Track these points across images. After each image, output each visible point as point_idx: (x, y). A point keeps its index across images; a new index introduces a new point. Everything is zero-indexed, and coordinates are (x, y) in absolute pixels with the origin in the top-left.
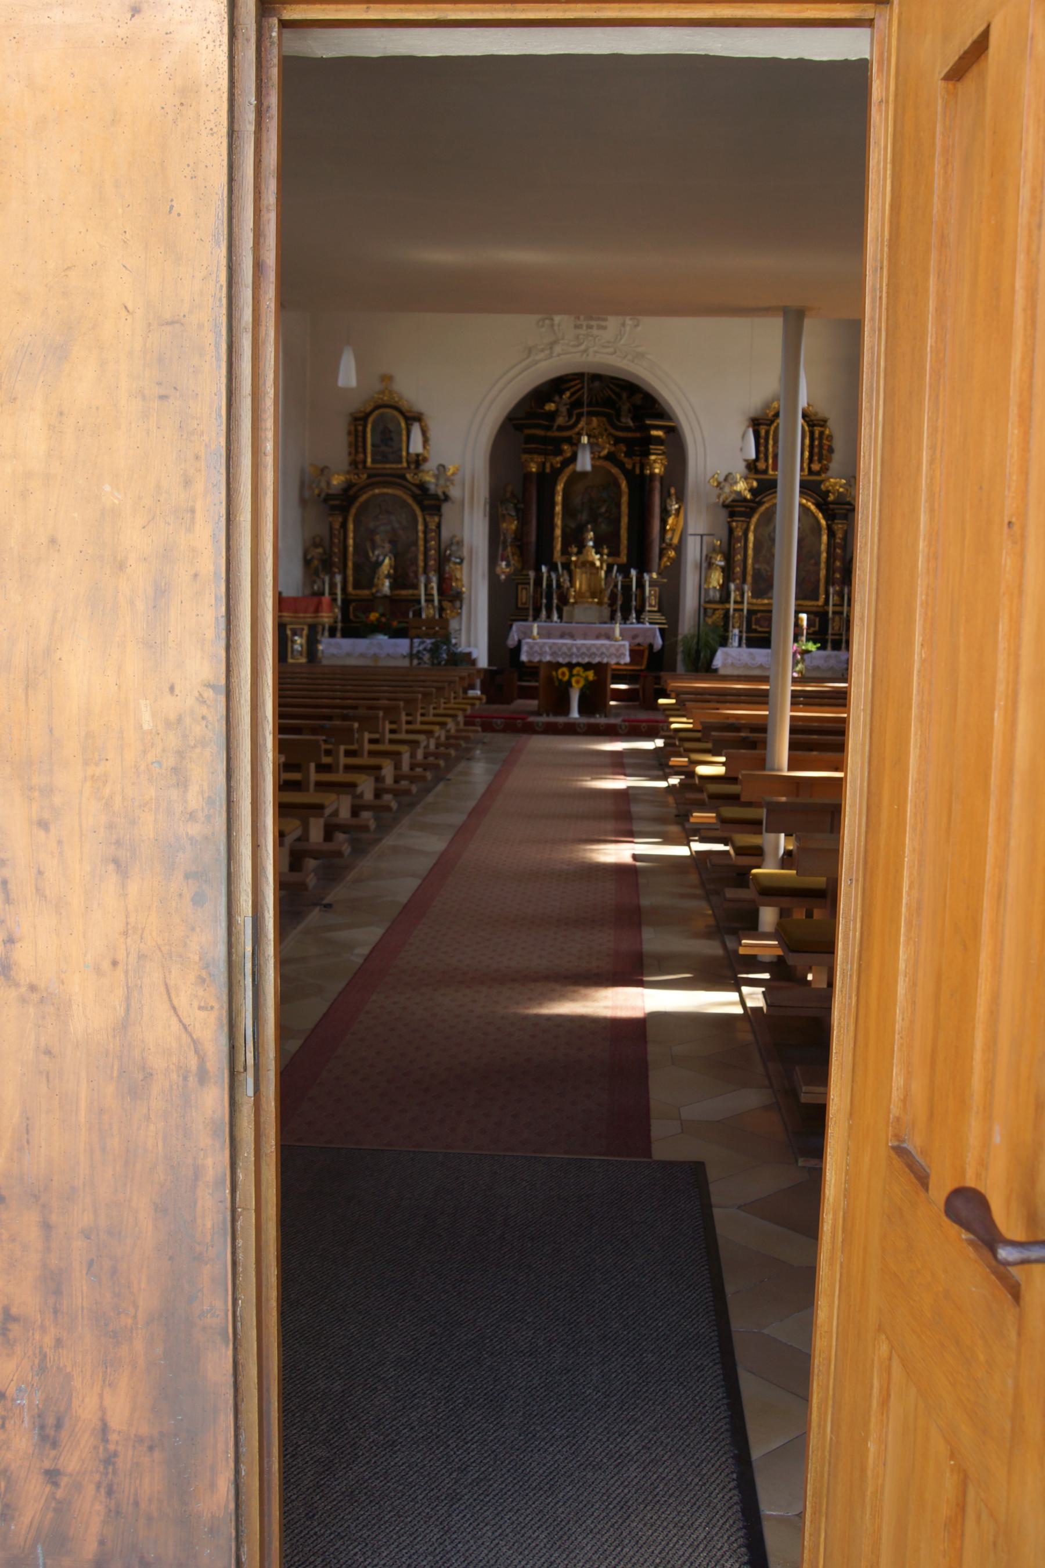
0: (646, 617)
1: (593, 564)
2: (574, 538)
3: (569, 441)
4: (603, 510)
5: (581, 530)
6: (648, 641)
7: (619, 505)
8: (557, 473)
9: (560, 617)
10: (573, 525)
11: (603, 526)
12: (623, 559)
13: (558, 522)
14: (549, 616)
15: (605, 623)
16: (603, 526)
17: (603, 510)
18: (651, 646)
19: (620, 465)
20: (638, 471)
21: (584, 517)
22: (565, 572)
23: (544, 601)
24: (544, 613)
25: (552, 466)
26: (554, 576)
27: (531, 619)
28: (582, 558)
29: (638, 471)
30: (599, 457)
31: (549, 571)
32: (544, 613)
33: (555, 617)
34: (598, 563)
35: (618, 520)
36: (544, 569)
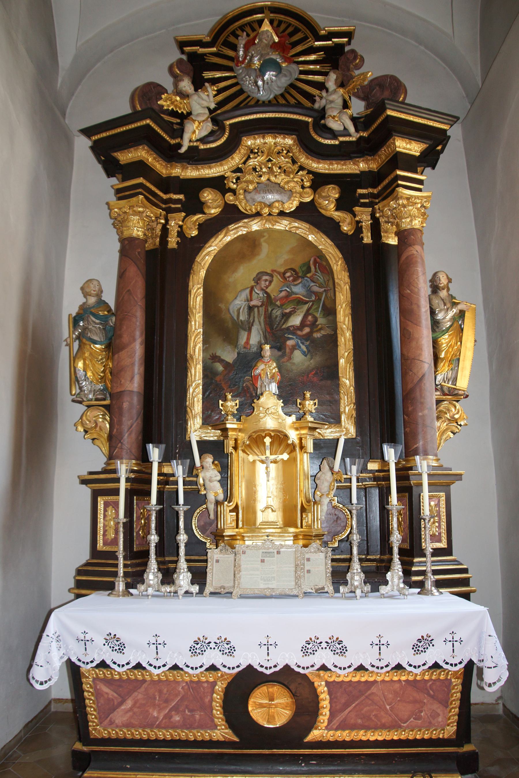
0: (426, 564)
1: (280, 438)
2: (233, 381)
3: (218, 184)
4: (296, 320)
5: (248, 361)
6: (464, 654)
7: (330, 312)
8: (192, 247)
9: (199, 577)
10: (229, 355)
11: (298, 356)
12: (347, 429)
13: (196, 347)
14: (168, 576)
15: (320, 592)
16: (298, 356)
17: (296, 320)
18: (470, 671)
19: (328, 227)
20: (367, 239)
21: (255, 337)
22: (209, 459)
23: (154, 538)
24: (152, 575)
25: (181, 234)
26: (178, 470)
27: (121, 586)
28: (250, 424)
29: (367, 239)
30: (282, 214)
31: (166, 459)
32: (152, 575)
33: (184, 578)
34: (293, 436)
35: (332, 340)
36: (155, 453)
